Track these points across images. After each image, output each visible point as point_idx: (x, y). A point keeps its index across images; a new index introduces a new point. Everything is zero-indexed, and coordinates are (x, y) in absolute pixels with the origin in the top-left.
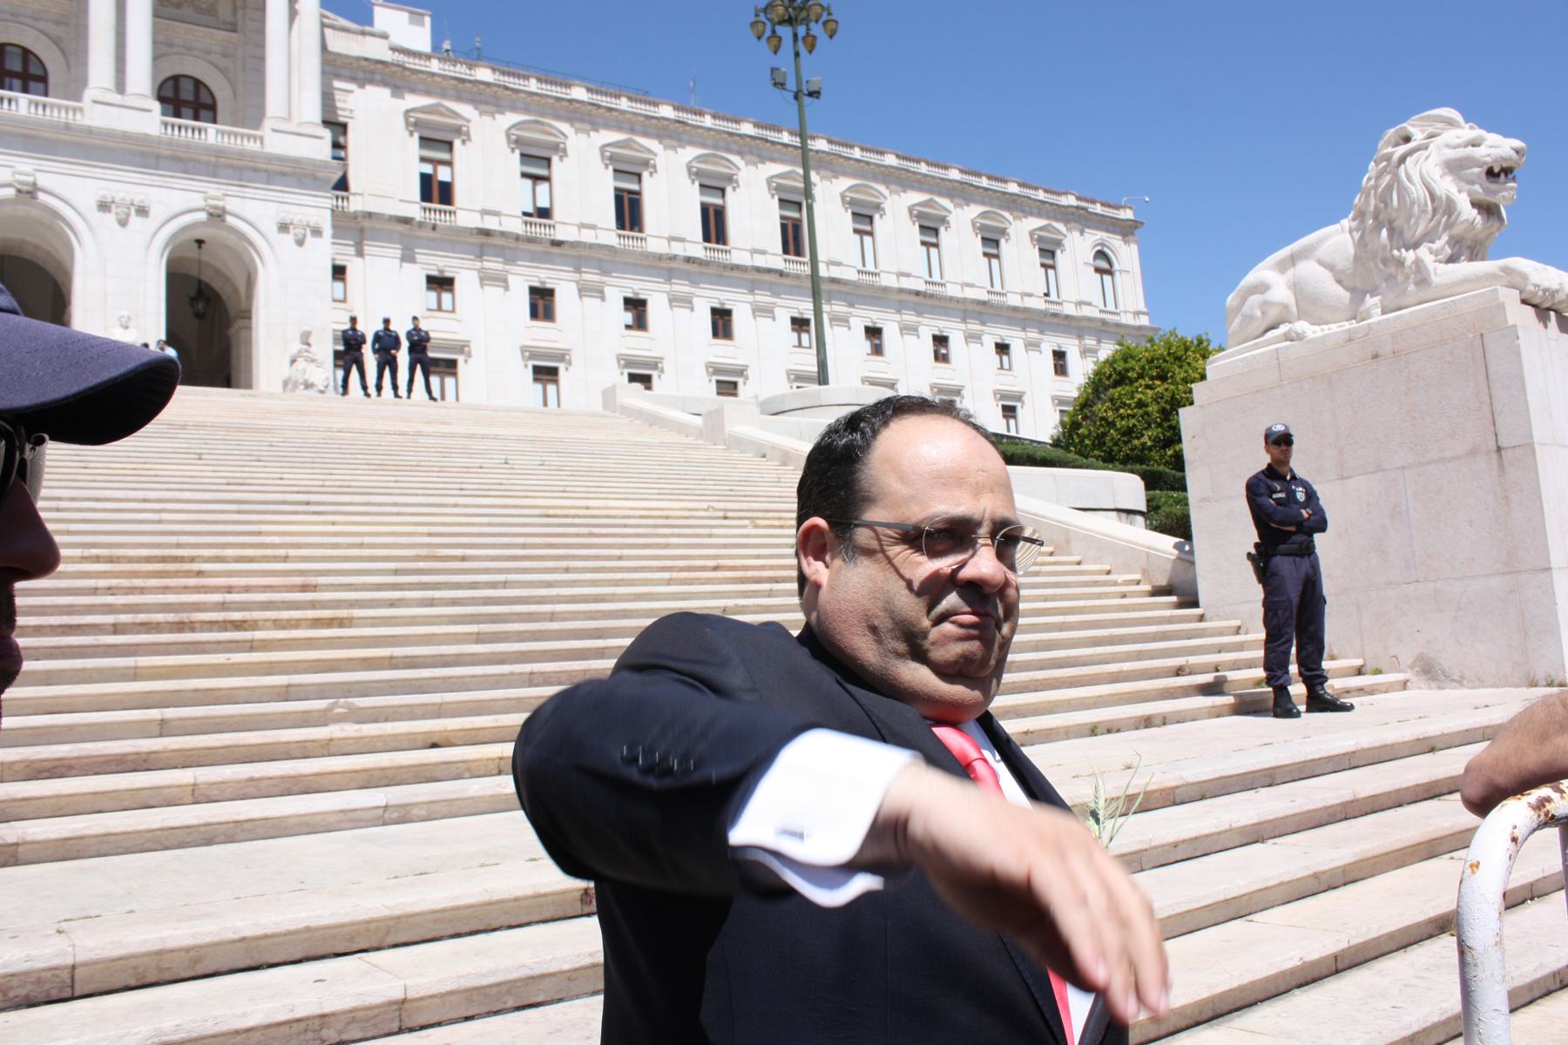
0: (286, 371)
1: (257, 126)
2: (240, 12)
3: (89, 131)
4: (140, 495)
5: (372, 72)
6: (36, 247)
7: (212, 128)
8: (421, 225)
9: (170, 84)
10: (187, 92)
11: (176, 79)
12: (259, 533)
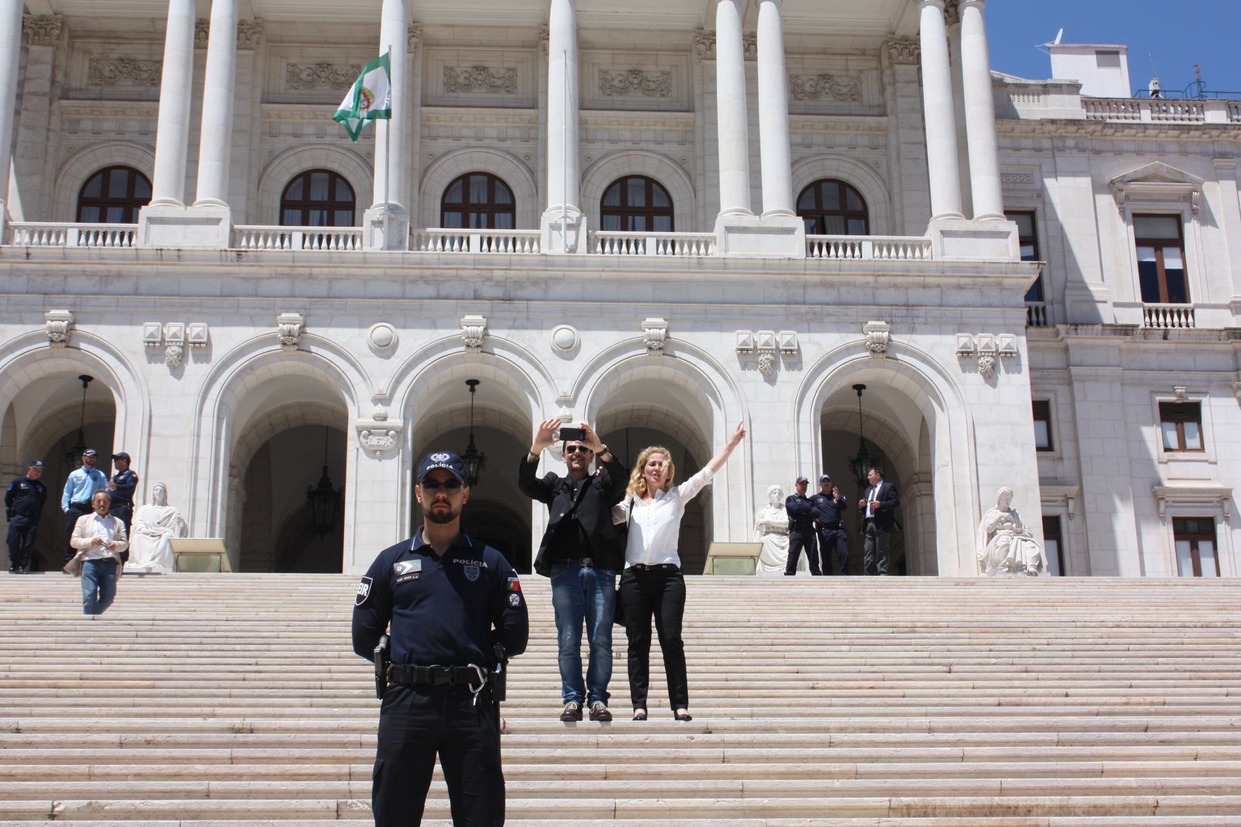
0: (981, 548)
1: (923, 235)
2: (889, 90)
3: (724, 265)
4: (924, 721)
5: (1062, 138)
6: (666, 415)
7: (867, 244)
8: (1146, 333)
9: (811, 192)
10: (830, 203)
11: (816, 186)
12: (1102, 773)
